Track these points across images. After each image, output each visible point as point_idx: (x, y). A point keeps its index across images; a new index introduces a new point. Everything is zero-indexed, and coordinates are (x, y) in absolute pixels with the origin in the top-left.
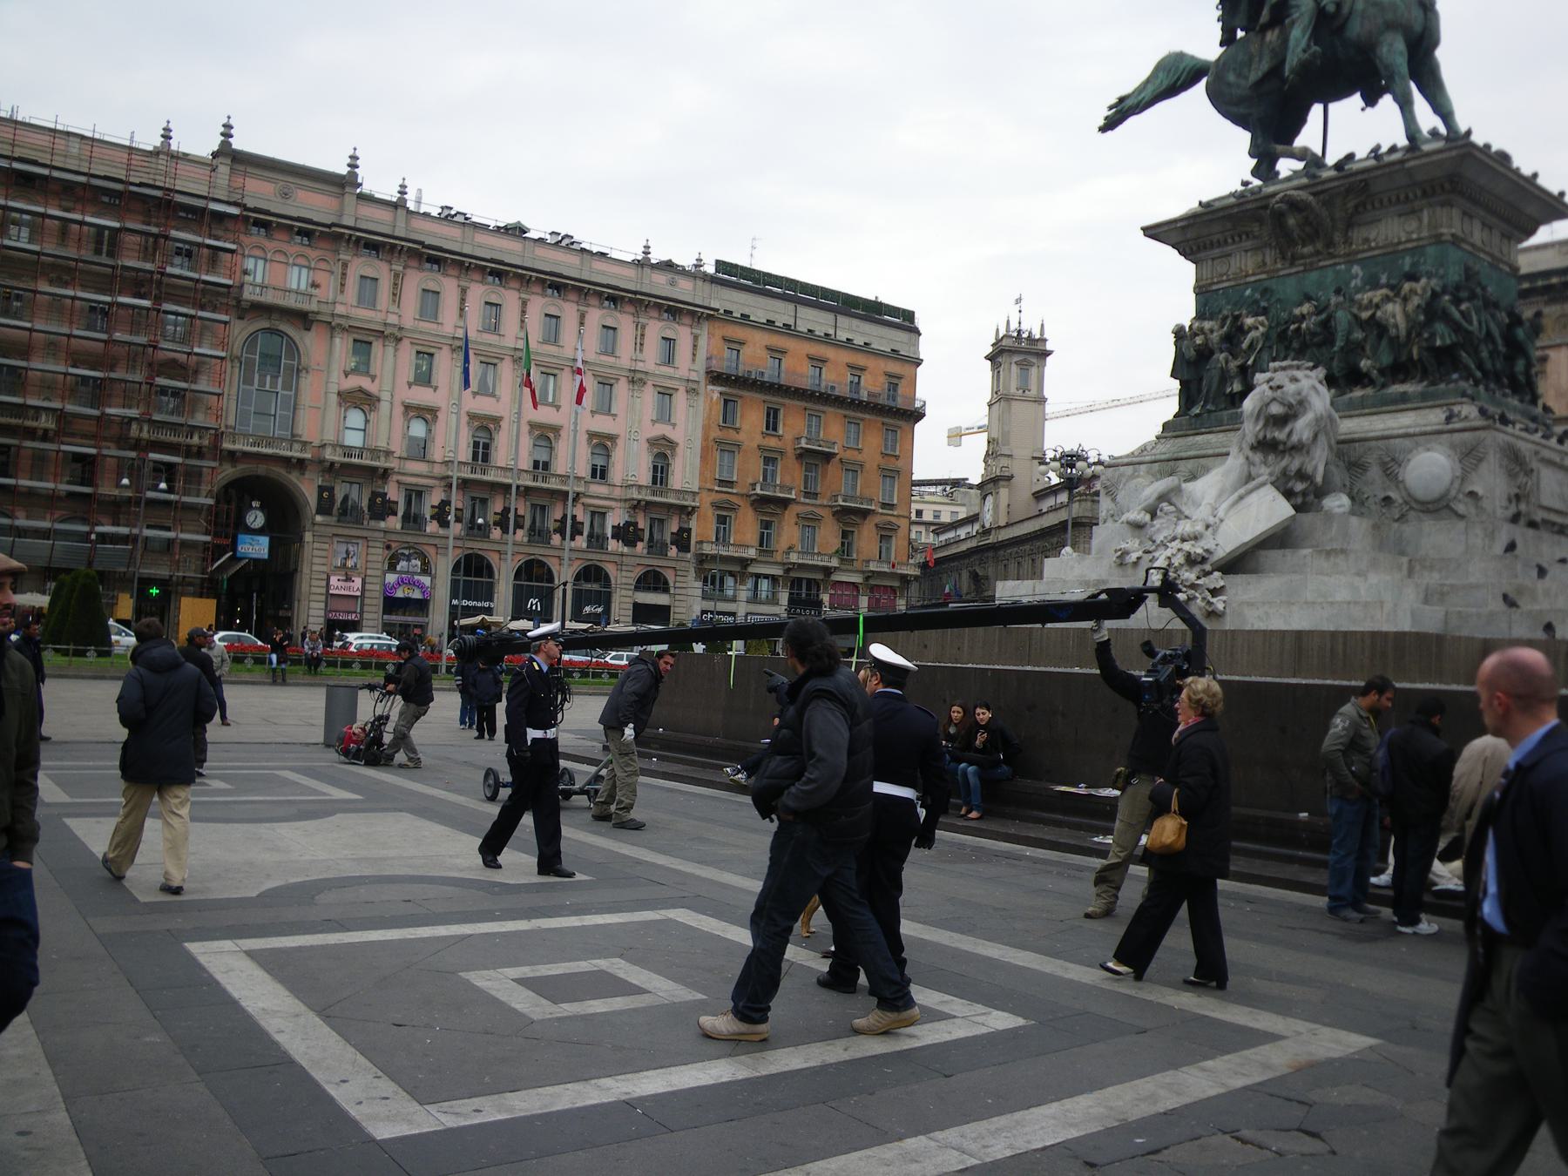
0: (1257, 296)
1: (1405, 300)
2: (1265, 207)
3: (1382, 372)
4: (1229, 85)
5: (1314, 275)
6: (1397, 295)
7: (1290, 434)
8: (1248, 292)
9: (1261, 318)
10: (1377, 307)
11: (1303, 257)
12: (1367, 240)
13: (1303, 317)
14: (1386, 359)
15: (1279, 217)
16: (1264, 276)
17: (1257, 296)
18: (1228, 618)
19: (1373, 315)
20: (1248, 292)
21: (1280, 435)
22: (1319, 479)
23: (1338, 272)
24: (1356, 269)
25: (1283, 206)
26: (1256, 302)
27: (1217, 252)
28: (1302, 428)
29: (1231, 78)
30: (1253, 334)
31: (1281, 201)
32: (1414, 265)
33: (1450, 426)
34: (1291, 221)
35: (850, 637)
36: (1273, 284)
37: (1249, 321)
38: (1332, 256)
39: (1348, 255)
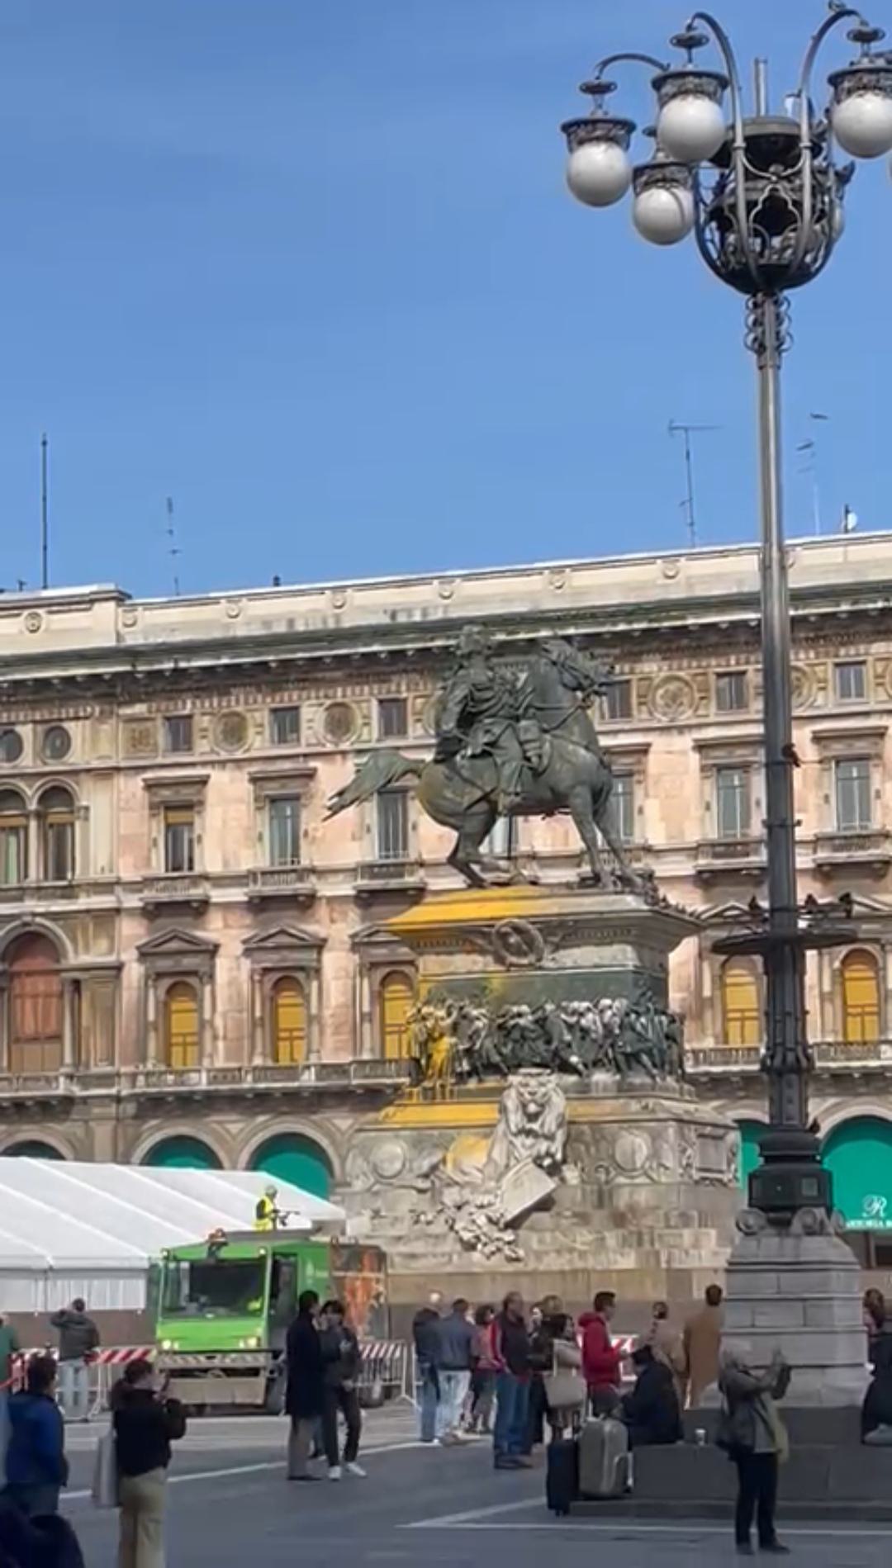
1: (602, 1012)
3: (586, 1066)
6: (596, 1006)
7: (542, 1125)
9: (483, 1011)
10: (581, 1015)
13: (520, 1015)
14: (591, 1057)
15: (504, 936)
19: (578, 1022)
21: (535, 1126)
22: (559, 1156)
25: (508, 929)
28: (549, 1121)
30: (479, 1024)
37: (475, 1013)
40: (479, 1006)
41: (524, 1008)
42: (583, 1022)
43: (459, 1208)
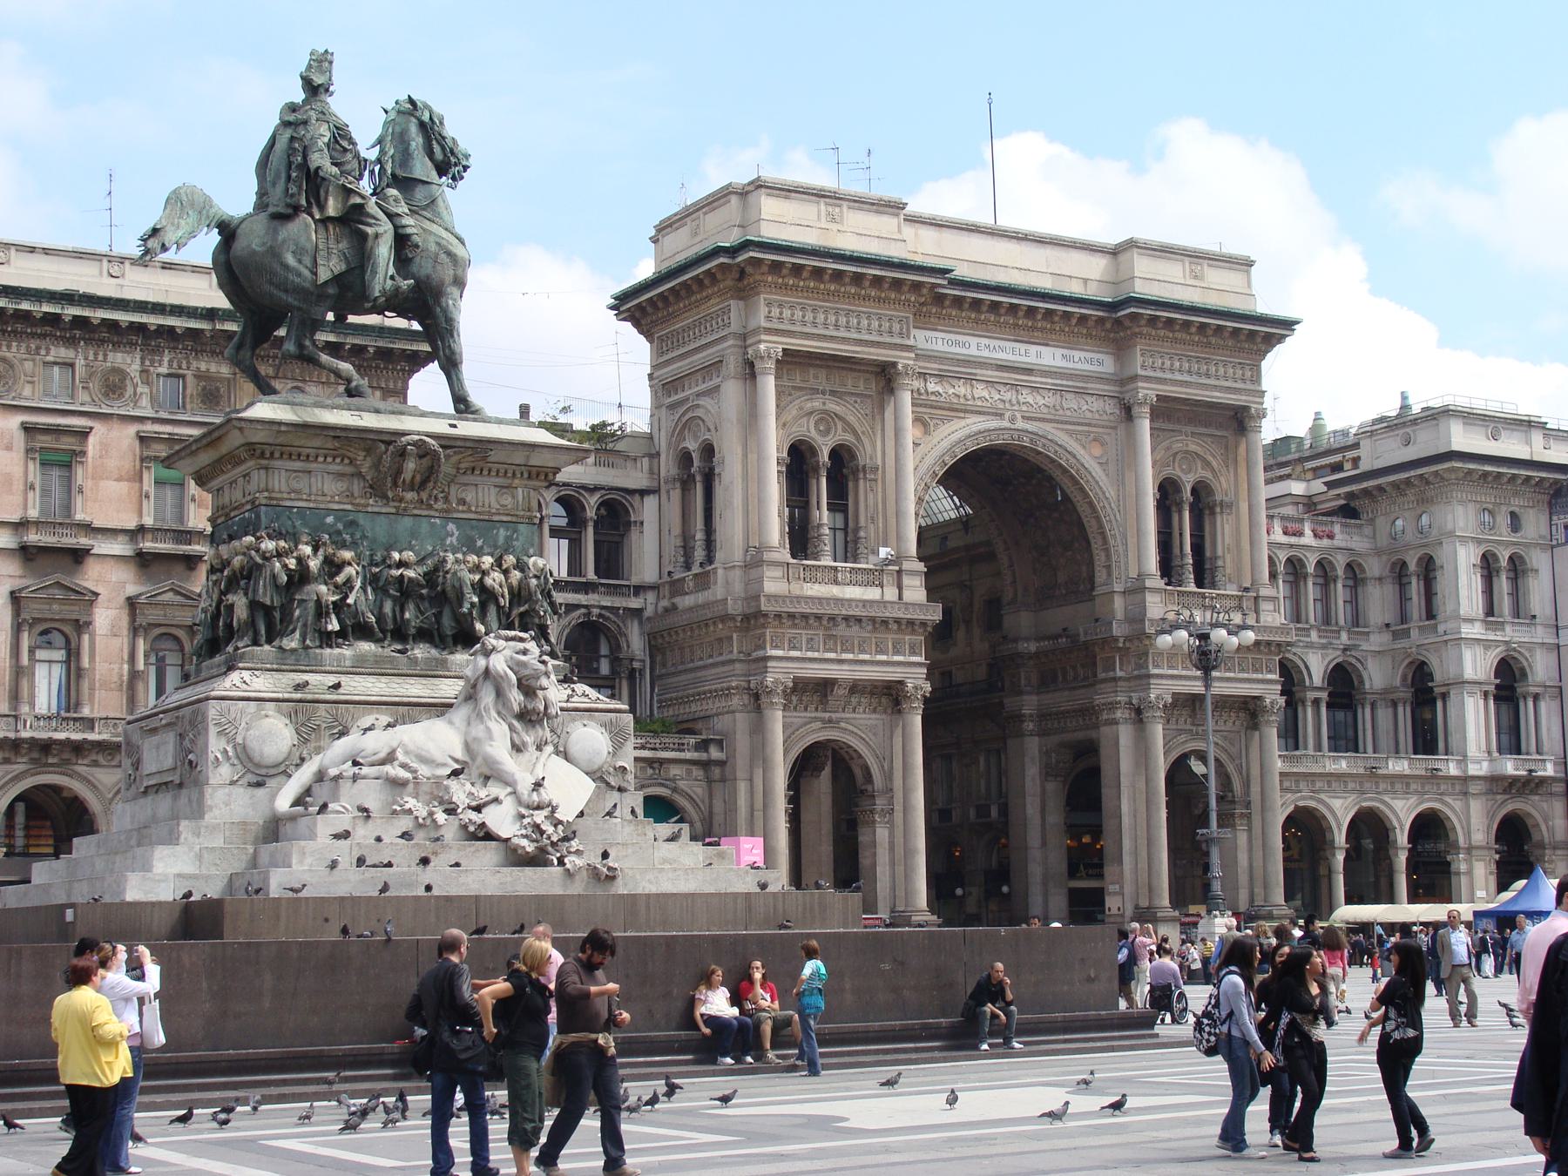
0: (340, 526)
2: (388, 443)
4: (286, 267)
5: (407, 522)
8: (330, 520)
12: (462, 502)
16: (349, 507)
17: (340, 526)
18: (619, 881)
20: (330, 520)
23: (433, 525)
24: (451, 527)
26: (339, 533)
27: (298, 465)
29: (290, 260)
31: (415, 444)
32: (508, 539)
33: (570, 705)
34: (410, 466)
35: (1065, 913)
36: (361, 519)
37: (347, 555)
38: (430, 507)
39: (447, 511)
40: (344, 546)
41: (409, 555)
42: (488, 581)
43: (478, 809)
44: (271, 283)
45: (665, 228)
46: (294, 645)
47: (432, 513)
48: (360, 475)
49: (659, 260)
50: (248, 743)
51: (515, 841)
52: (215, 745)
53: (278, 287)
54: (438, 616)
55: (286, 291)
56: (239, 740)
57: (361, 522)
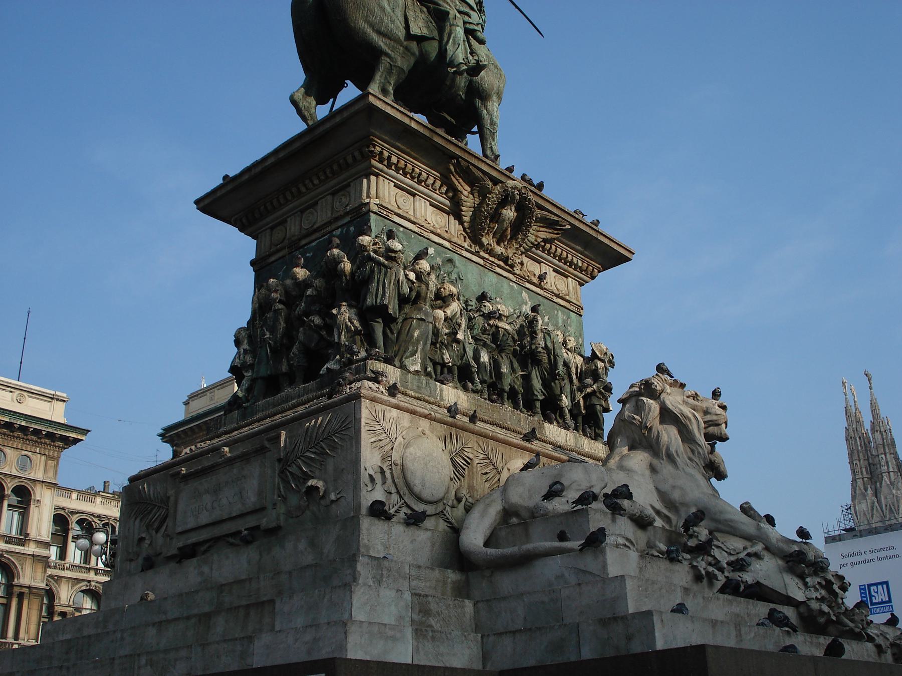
2: (496, 182)
4: (383, 9)
11: (491, 253)
44: (367, 21)
45: (193, 397)
46: (418, 367)
47: (511, 276)
48: (458, 217)
49: (187, 411)
50: (409, 465)
51: (815, 605)
52: (370, 459)
53: (372, 26)
54: (527, 379)
55: (379, 33)
56: (396, 456)
57: (457, 264)
